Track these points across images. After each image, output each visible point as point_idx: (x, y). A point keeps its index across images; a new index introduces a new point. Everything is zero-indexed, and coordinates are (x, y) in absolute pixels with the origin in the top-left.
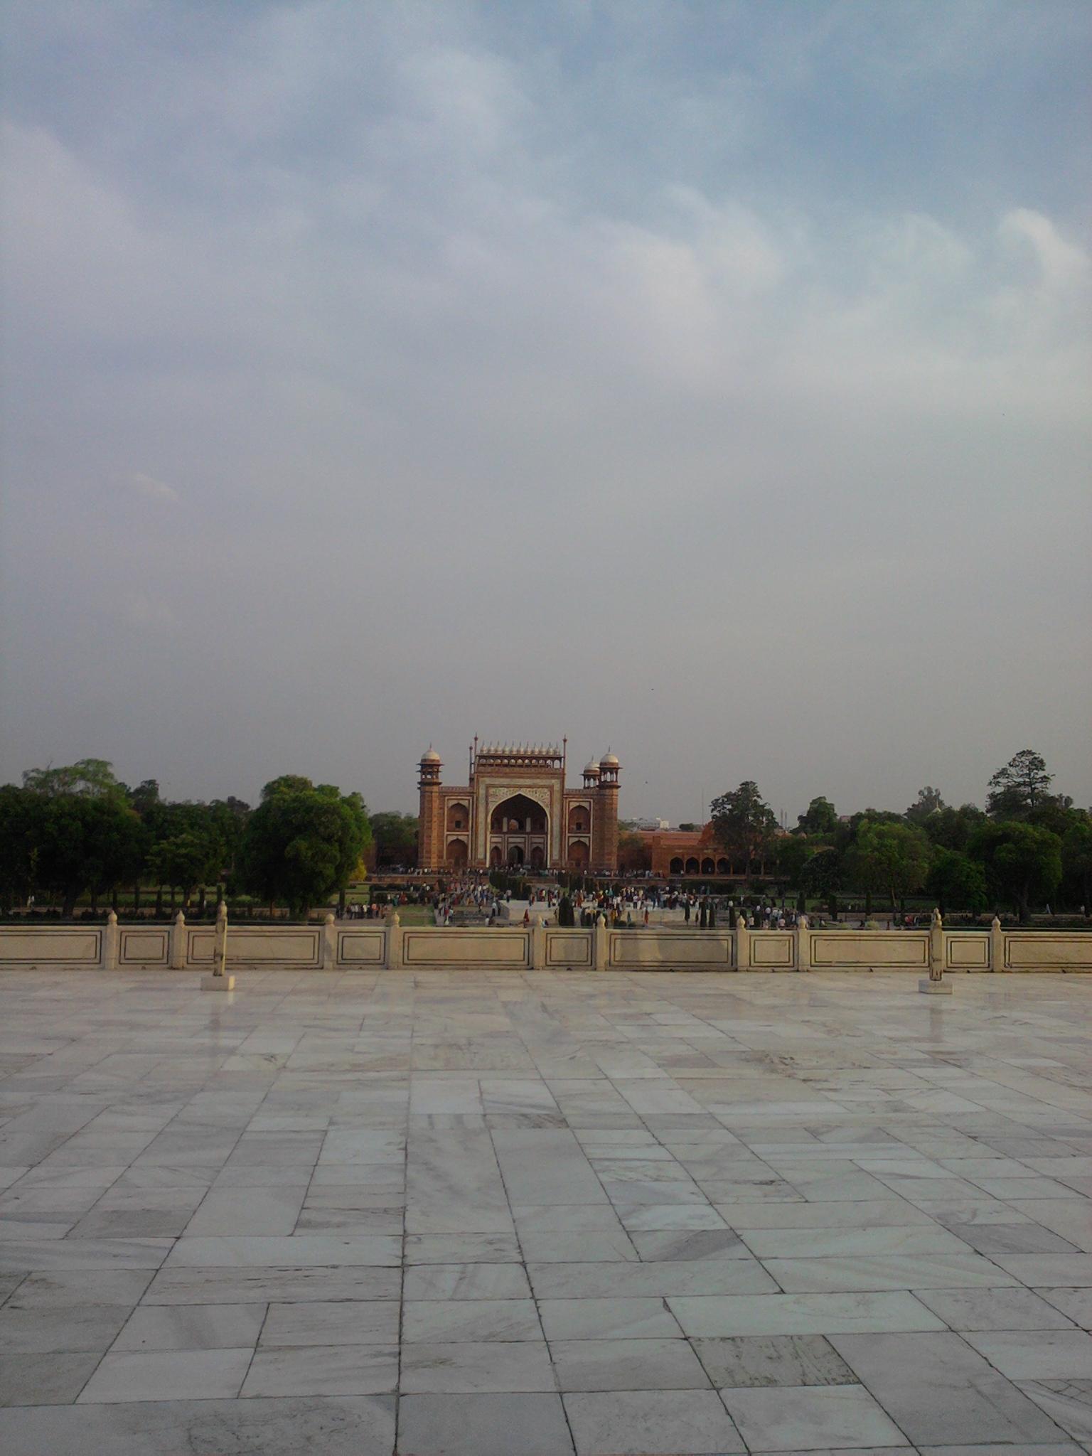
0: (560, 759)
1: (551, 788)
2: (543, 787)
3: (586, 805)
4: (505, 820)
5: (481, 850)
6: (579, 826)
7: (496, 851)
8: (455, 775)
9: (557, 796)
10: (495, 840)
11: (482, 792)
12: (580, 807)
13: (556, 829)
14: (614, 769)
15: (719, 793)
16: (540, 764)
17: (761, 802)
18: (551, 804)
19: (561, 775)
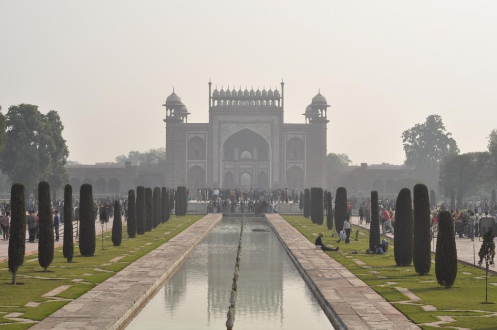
3: (300, 137)
8: (198, 113)
10: (227, 166)
16: (267, 104)
17: (445, 133)
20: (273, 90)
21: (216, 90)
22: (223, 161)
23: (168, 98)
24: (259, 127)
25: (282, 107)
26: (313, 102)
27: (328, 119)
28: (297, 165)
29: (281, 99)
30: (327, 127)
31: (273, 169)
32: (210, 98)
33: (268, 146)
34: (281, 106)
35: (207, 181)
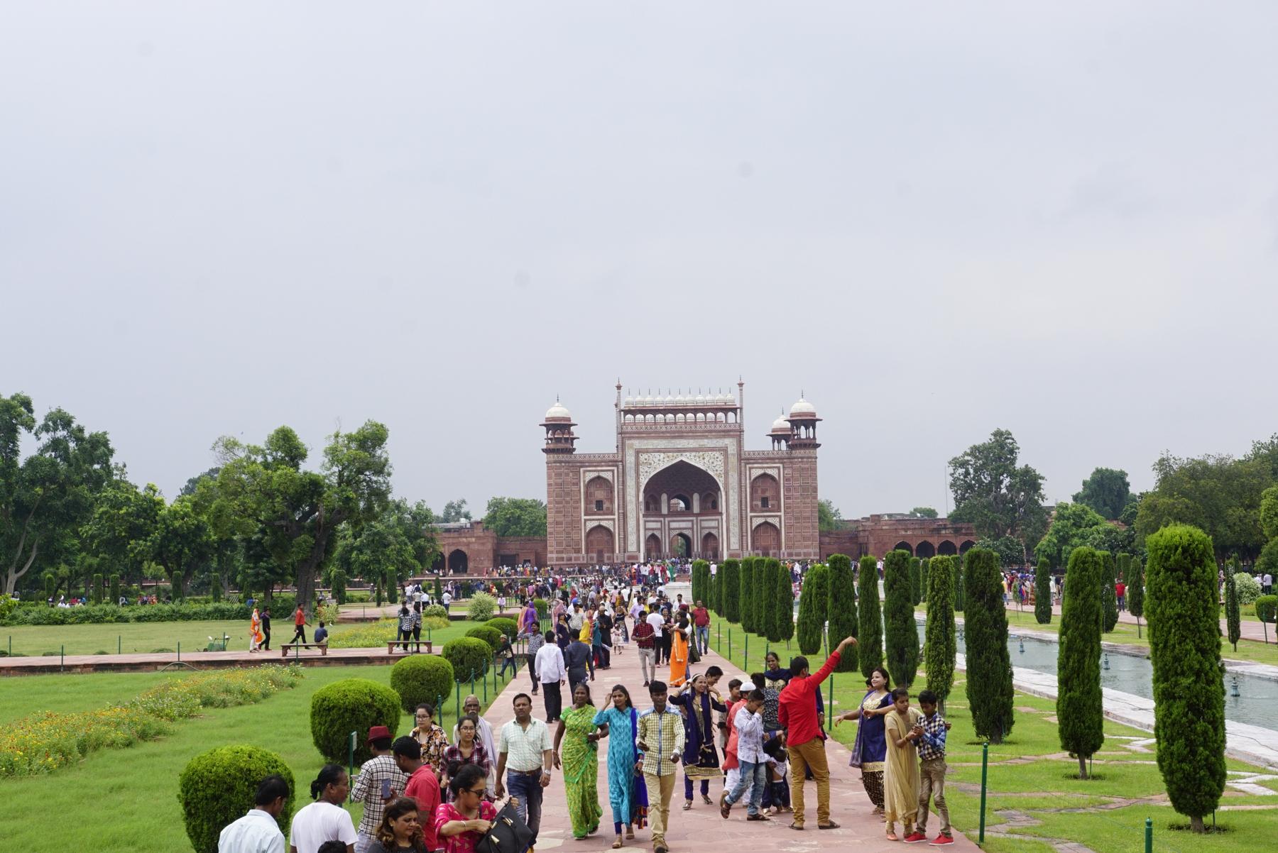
0: (734, 410)
1: (724, 450)
2: (713, 449)
4: (664, 497)
5: (632, 539)
6: (765, 501)
7: (653, 541)
9: (733, 460)
10: (650, 525)
11: (630, 459)
12: (765, 476)
13: (734, 507)
14: (809, 421)
15: (960, 449)
18: (726, 473)
19: (738, 433)
25: (740, 425)
28: (770, 520)
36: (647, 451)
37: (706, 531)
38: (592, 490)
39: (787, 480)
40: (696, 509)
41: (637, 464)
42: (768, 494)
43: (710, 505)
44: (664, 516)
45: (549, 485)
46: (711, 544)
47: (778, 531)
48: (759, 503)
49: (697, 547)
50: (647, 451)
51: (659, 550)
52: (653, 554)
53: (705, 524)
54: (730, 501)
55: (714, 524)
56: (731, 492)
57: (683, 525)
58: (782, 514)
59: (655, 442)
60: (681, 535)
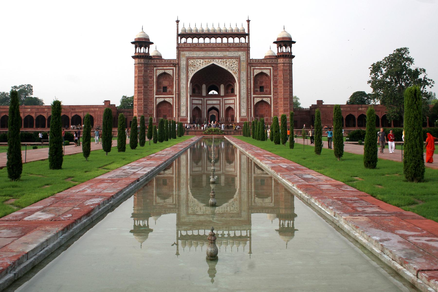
1: (238, 58)
3: (267, 72)
4: (204, 86)
5: (183, 109)
7: (196, 112)
9: (244, 65)
10: (195, 102)
11: (183, 63)
12: (262, 74)
19: (246, 48)
20: (240, 28)
21: (184, 27)
22: (190, 96)
23: (137, 36)
24: (226, 63)
26: (278, 39)
27: (293, 54)
28: (265, 99)
29: (247, 37)
30: (293, 62)
31: (240, 104)
32: (178, 35)
33: (235, 82)
34: (247, 42)
35: (174, 116)
36: (193, 58)
37: (228, 106)
38: (161, 80)
39: (274, 76)
40: (222, 93)
41: (187, 66)
42: (263, 84)
43: (230, 91)
44: (204, 97)
45: (135, 77)
46: (230, 112)
47: (270, 106)
48: (259, 90)
49: (222, 115)
50: (193, 58)
51: (200, 116)
52: (197, 118)
53: (227, 102)
54: (241, 87)
55: (232, 102)
56: (242, 83)
57: (215, 102)
58: (272, 96)
59: (198, 53)
60: (213, 108)
